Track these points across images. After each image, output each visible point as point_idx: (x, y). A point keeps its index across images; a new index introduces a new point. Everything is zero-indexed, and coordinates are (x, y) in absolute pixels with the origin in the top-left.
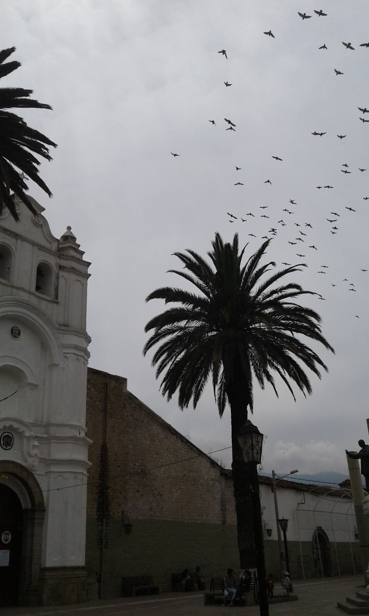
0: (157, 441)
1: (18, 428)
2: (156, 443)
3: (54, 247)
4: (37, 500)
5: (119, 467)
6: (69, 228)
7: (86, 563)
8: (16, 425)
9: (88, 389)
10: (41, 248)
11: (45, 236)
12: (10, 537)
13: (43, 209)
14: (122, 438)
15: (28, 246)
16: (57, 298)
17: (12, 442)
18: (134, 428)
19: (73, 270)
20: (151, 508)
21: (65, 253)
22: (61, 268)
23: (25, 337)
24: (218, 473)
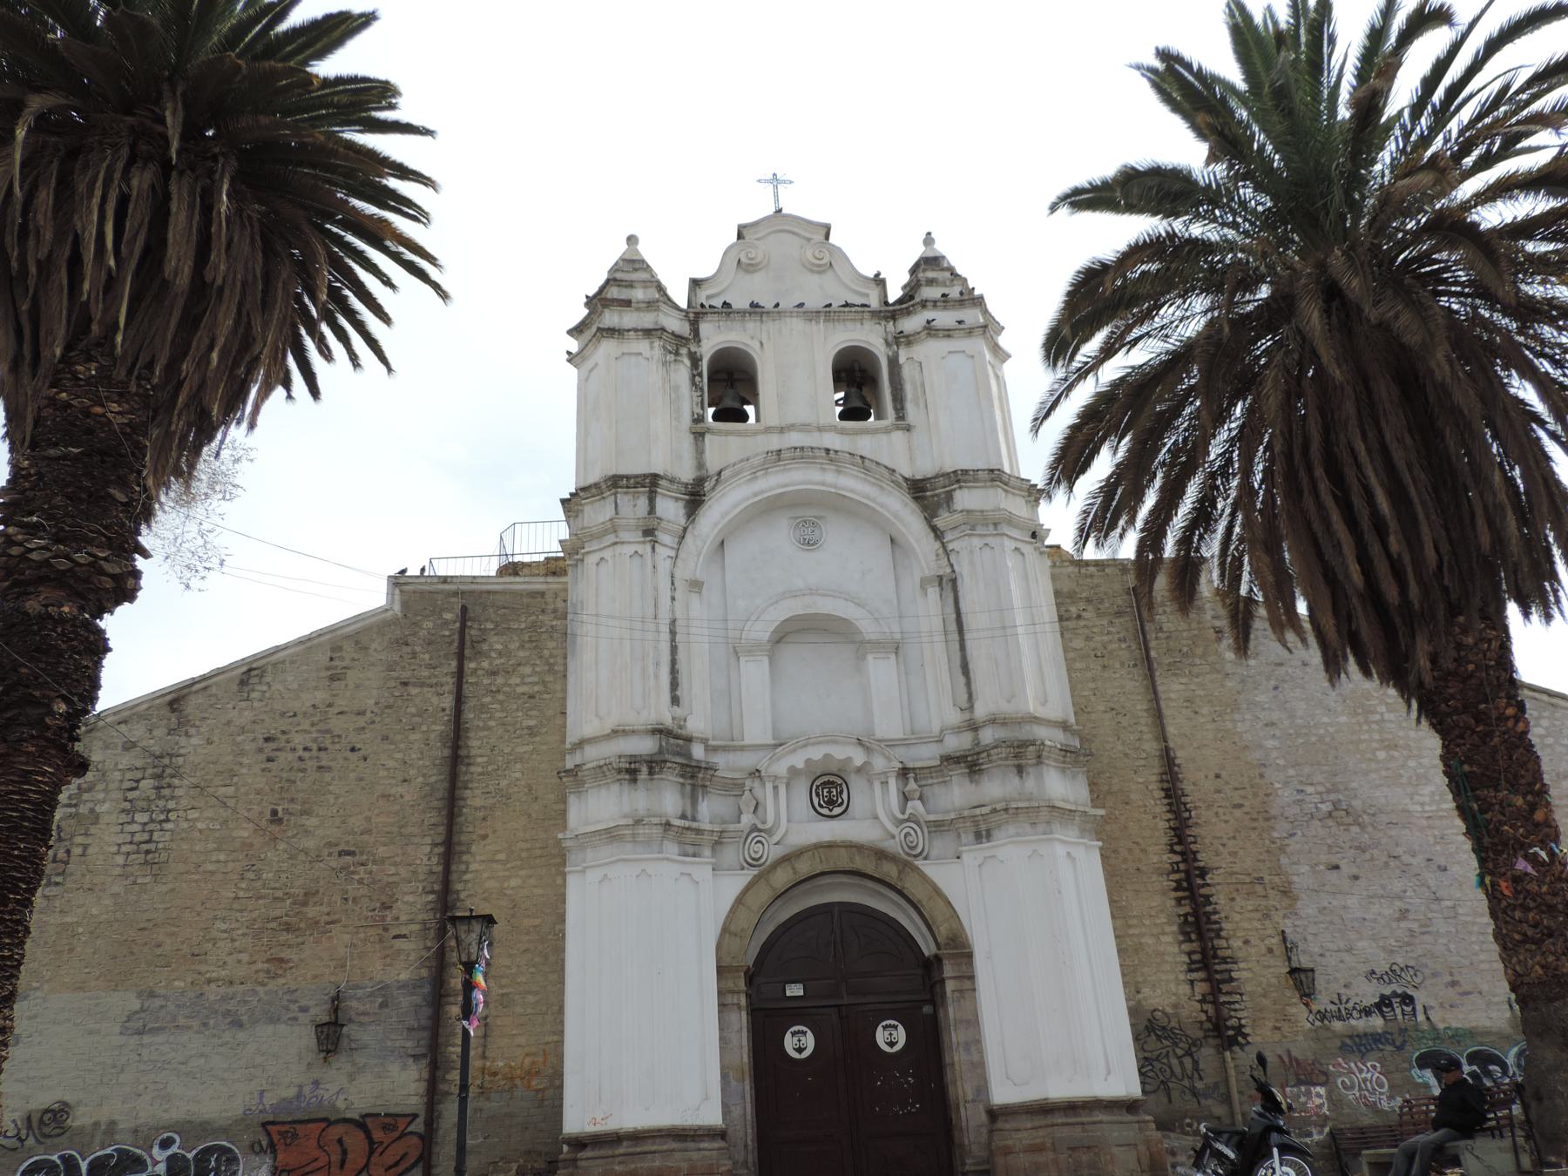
0: (1383, 709)
1: (849, 759)
2: (1377, 717)
4: (943, 931)
5: (1240, 806)
6: (929, 240)
7: (1143, 1091)
8: (839, 753)
10: (828, 313)
11: (847, 287)
12: (901, 1035)
13: (827, 230)
14: (1229, 725)
15: (797, 324)
17: (845, 796)
18: (1276, 688)
19: (930, 330)
20: (1404, 914)
23: (837, 537)
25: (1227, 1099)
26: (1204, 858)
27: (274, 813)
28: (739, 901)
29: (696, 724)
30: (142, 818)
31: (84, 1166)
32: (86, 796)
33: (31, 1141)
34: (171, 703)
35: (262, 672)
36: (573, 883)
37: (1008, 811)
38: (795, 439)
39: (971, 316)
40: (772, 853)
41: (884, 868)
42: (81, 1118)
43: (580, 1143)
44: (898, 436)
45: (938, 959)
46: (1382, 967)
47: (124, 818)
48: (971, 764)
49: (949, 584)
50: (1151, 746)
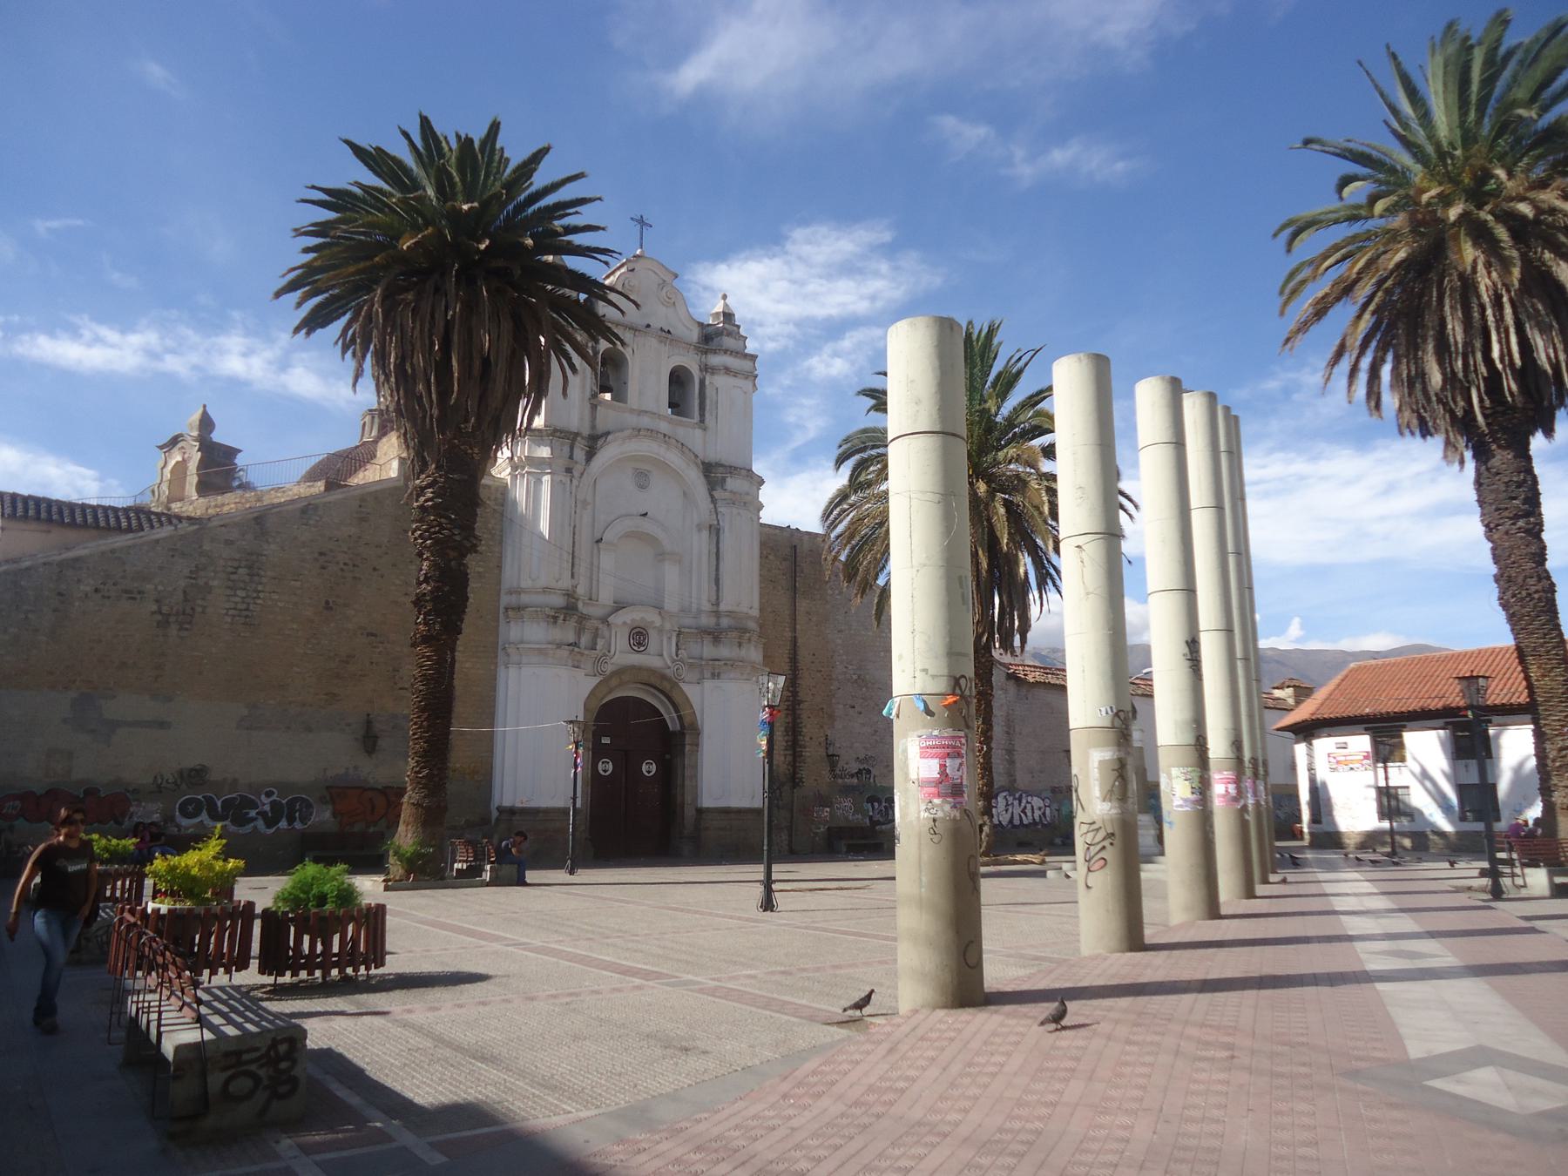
3: (694, 335)
4: (687, 721)
9: (763, 557)
12: (654, 768)
16: (702, 421)
21: (713, 345)
22: (705, 368)
24: (1003, 679)
25: (792, 810)
26: (801, 696)
27: (327, 603)
28: (592, 693)
29: (581, 590)
30: (239, 593)
31: (219, 804)
32: (202, 573)
33: (184, 786)
34: (256, 519)
35: (316, 508)
36: (501, 672)
37: (731, 663)
38: (646, 421)
39: (746, 365)
40: (609, 669)
41: (664, 685)
42: (214, 776)
43: (512, 811)
44: (698, 432)
45: (682, 734)
46: (862, 756)
47: (229, 592)
48: (716, 636)
49: (716, 531)
50: (788, 634)
